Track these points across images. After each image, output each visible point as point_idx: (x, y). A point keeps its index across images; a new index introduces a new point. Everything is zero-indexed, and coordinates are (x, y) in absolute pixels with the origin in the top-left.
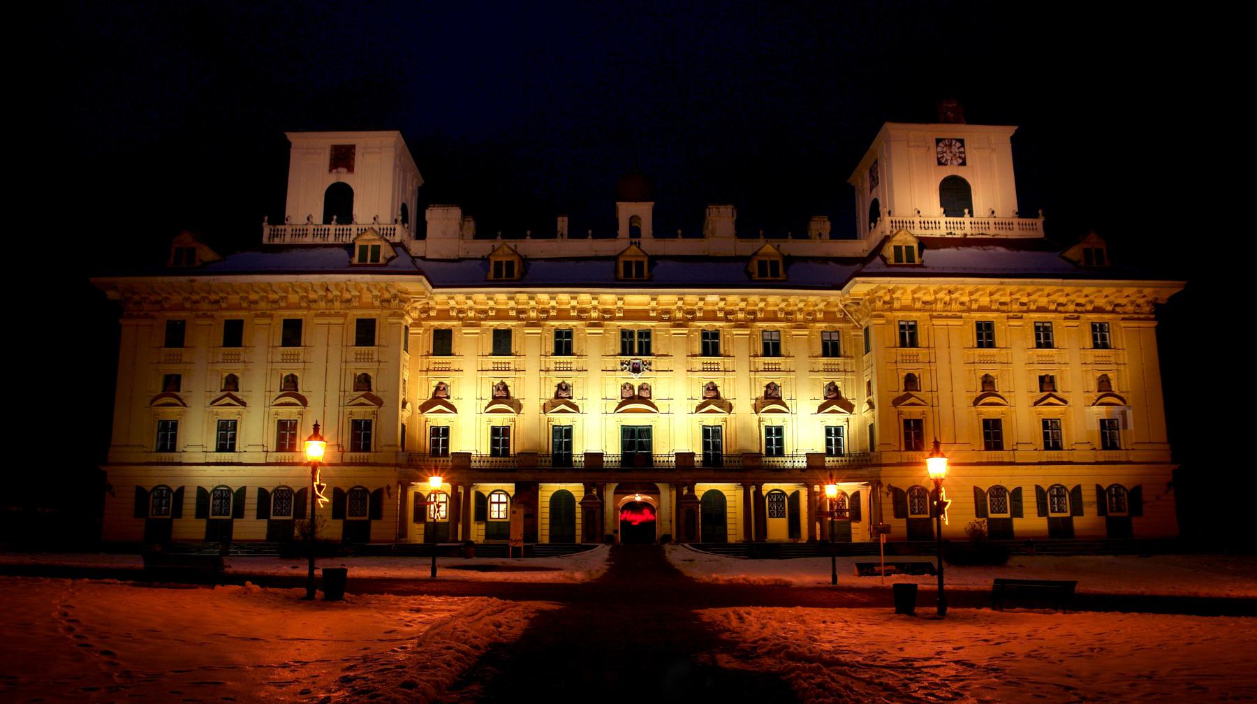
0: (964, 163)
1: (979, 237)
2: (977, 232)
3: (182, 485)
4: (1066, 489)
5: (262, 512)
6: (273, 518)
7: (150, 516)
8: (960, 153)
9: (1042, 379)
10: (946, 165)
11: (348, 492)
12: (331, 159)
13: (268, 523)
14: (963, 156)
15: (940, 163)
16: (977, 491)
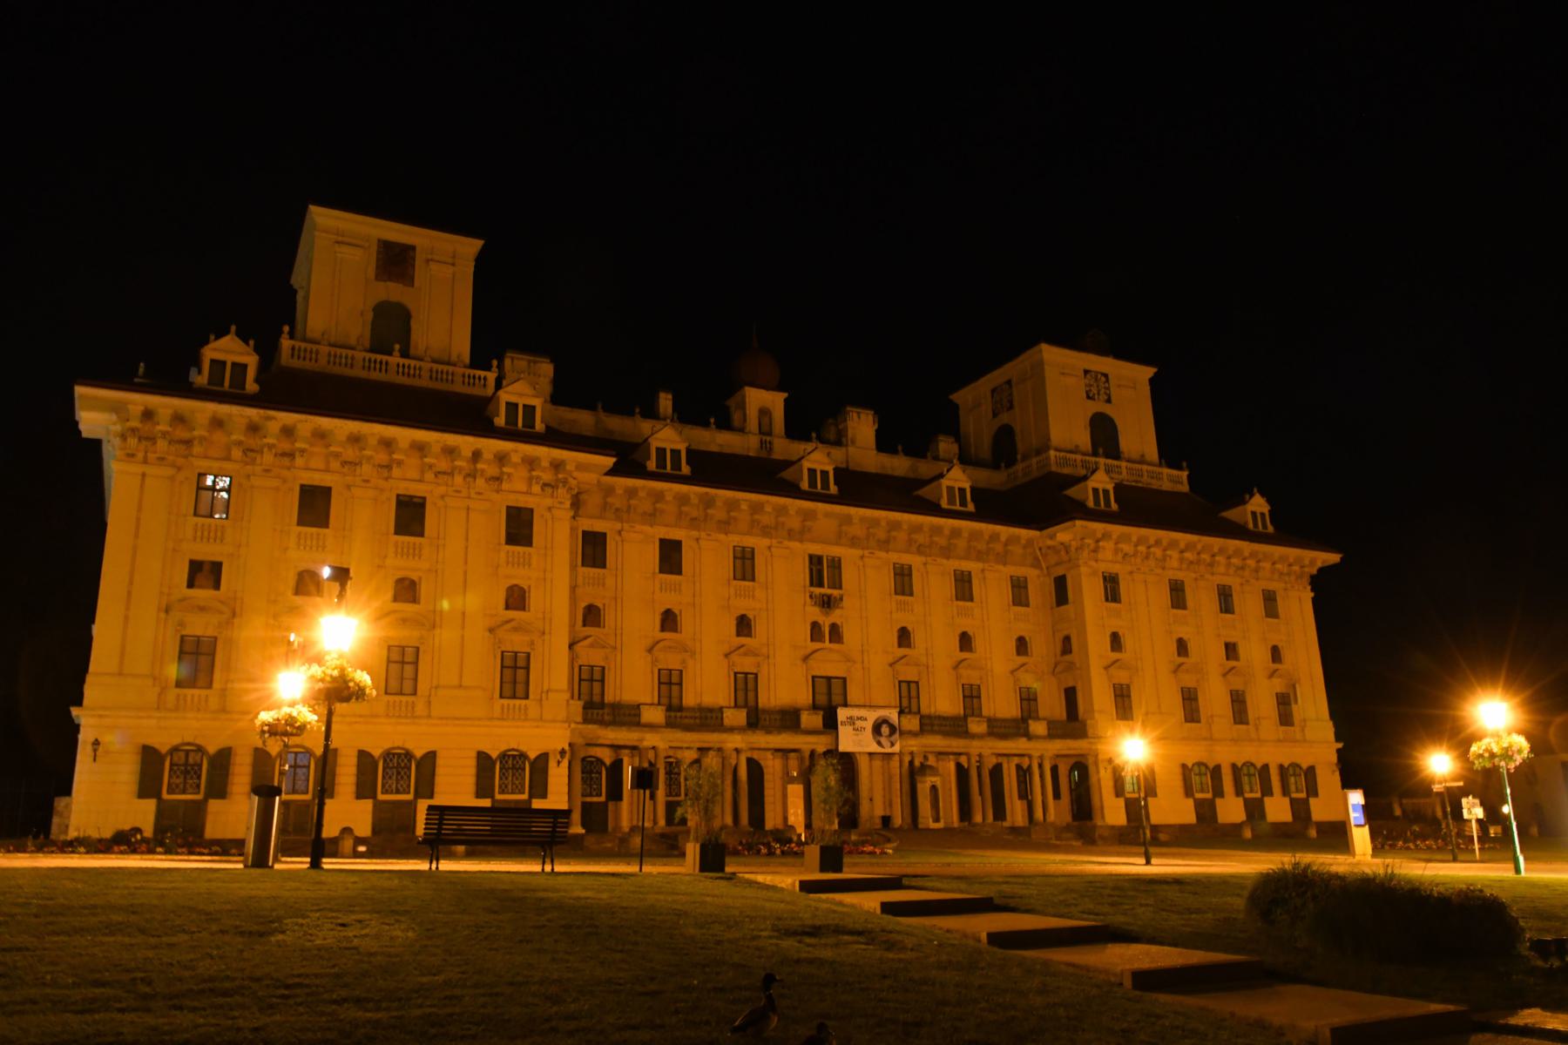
0: (1109, 401)
1: (1133, 484)
2: (1135, 478)
3: (1216, 763)
4: (1301, 768)
5: (364, 789)
6: (381, 797)
7: (165, 796)
8: (1105, 388)
9: (1227, 645)
10: (1094, 400)
11: (499, 757)
12: (378, 260)
13: (374, 806)
14: (1108, 392)
15: (1088, 397)
16: (1184, 766)
